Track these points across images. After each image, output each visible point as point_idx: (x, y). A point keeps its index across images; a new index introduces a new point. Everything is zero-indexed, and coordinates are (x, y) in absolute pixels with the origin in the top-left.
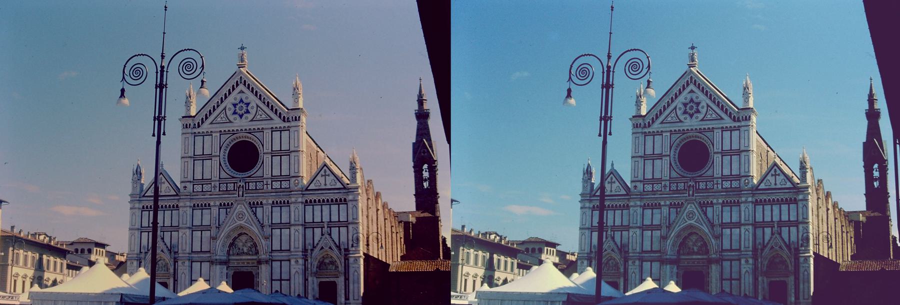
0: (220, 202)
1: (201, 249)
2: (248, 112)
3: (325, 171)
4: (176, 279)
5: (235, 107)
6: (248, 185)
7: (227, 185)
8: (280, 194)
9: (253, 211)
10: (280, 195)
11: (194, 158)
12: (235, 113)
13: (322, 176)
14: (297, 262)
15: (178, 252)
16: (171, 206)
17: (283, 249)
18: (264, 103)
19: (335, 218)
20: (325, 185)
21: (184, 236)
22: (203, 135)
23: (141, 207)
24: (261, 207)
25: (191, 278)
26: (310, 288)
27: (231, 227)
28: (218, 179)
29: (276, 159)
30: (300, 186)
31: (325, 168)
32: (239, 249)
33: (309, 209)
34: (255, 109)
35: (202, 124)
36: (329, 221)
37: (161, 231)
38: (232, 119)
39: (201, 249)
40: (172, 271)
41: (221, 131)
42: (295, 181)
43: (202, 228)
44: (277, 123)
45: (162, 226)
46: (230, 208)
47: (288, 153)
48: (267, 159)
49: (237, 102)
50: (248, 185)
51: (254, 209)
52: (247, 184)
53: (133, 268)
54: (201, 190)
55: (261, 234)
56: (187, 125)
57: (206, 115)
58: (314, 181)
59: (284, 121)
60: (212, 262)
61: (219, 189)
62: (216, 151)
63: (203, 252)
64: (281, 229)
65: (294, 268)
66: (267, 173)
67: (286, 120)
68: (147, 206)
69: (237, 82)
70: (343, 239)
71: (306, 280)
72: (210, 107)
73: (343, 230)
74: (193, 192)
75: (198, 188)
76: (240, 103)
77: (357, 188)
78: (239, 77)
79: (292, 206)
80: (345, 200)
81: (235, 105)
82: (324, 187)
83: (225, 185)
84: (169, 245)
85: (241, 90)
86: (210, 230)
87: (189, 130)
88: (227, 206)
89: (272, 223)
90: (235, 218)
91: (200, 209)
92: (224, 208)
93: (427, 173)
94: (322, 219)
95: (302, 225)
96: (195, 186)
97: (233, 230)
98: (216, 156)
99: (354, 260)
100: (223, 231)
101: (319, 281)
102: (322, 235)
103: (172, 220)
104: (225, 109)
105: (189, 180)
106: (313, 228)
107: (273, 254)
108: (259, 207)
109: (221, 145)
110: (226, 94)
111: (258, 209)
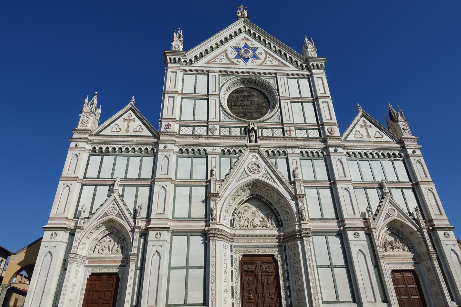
1: (190, 213)
5: (238, 52)
10: (311, 144)
12: (239, 56)
17: (325, 216)
21: (163, 191)
22: (197, 73)
25: (170, 264)
27: (241, 182)
31: (363, 118)
35: (195, 62)
38: (235, 60)
39: (190, 213)
41: (221, 72)
44: (292, 69)
51: (273, 161)
52: (260, 130)
53: (54, 244)
54: (191, 133)
56: (175, 59)
60: (212, 233)
63: (193, 218)
64: (317, 188)
65: (355, 245)
68: (101, 148)
76: (243, 48)
81: (238, 49)
82: (368, 139)
83: (228, 129)
85: (245, 37)
99: (445, 234)
100: (227, 187)
101: (390, 270)
103: (140, 169)
104: (225, 52)
106: (365, 188)
111: (278, 161)
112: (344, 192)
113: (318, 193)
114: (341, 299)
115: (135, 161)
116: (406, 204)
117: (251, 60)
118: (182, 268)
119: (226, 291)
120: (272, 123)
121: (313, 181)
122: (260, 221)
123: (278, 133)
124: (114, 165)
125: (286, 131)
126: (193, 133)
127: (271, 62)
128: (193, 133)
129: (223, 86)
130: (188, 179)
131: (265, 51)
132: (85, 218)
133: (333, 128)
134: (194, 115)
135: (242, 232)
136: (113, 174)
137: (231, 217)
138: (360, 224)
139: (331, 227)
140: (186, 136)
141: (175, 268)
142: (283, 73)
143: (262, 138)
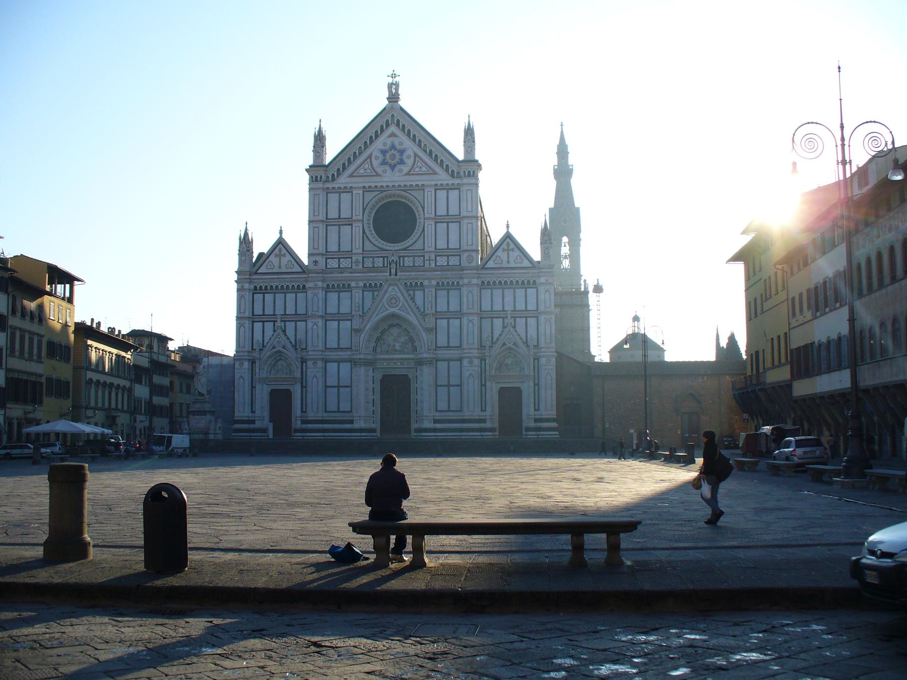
0: (365, 282)
1: (339, 344)
2: (402, 162)
3: (508, 245)
4: (304, 385)
6: (403, 260)
7: (373, 260)
8: (447, 272)
9: (410, 295)
11: (326, 222)
12: (384, 163)
13: (504, 250)
14: (471, 362)
15: (306, 349)
16: (296, 286)
18: (425, 151)
19: (521, 306)
20: (508, 262)
21: (315, 327)
23: (252, 287)
24: (420, 290)
26: (487, 396)
28: (361, 251)
29: (442, 227)
30: (474, 264)
32: (389, 345)
33: (487, 293)
34: (412, 159)
35: (338, 176)
36: (513, 309)
37: (282, 321)
38: (380, 170)
40: (299, 375)
41: (364, 187)
42: (469, 256)
43: (339, 317)
44: (443, 178)
45: (283, 313)
46: (379, 291)
47: (458, 219)
48: (430, 227)
49: (387, 148)
50: (403, 260)
51: (411, 292)
53: (244, 371)
55: (421, 325)
56: (317, 177)
57: (344, 164)
58: (494, 257)
59: (453, 176)
61: (363, 265)
62: (357, 214)
63: (341, 348)
64: (448, 319)
65: (468, 370)
66: (429, 246)
67: (455, 175)
69: (387, 121)
70: (532, 332)
71: (483, 385)
72: (350, 154)
73: (532, 322)
74: (326, 268)
75: (333, 264)
77: (552, 268)
78: (390, 115)
79: (464, 291)
80: (534, 282)
81: (384, 152)
82: (507, 266)
83: (371, 259)
84: (293, 340)
86: (351, 320)
87: (320, 185)
88: (372, 288)
89: (436, 311)
90: (385, 304)
91: (336, 292)
92: (371, 291)
93: (568, 247)
94: (503, 307)
95: (478, 314)
96: (328, 260)
97: (384, 320)
98: (358, 220)
102: (504, 327)
103: (296, 305)
104: (370, 157)
105: (321, 252)
106: (492, 318)
107: (437, 352)
108: (418, 290)
109: (365, 205)
110: (371, 137)
111: (416, 292)
112: (468, 323)
113: (448, 324)
114: (452, 409)
115: (290, 297)
116: (526, 332)
117: (398, 167)
118: (334, 387)
119: (367, 402)
120: (414, 250)
121: (445, 312)
122: (400, 346)
123: (419, 261)
124: (275, 302)
125: (427, 260)
126: (339, 265)
127: (420, 168)
128: (339, 265)
129: (367, 206)
130: (336, 314)
131: (414, 153)
132: (260, 350)
133: (472, 256)
134: (339, 245)
135: (382, 357)
136: (274, 311)
137: (374, 345)
138: (475, 353)
139: (455, 354)
140: (332, 271)
141: (330, 387)
142: (431, 186)
143: (405, 269)
